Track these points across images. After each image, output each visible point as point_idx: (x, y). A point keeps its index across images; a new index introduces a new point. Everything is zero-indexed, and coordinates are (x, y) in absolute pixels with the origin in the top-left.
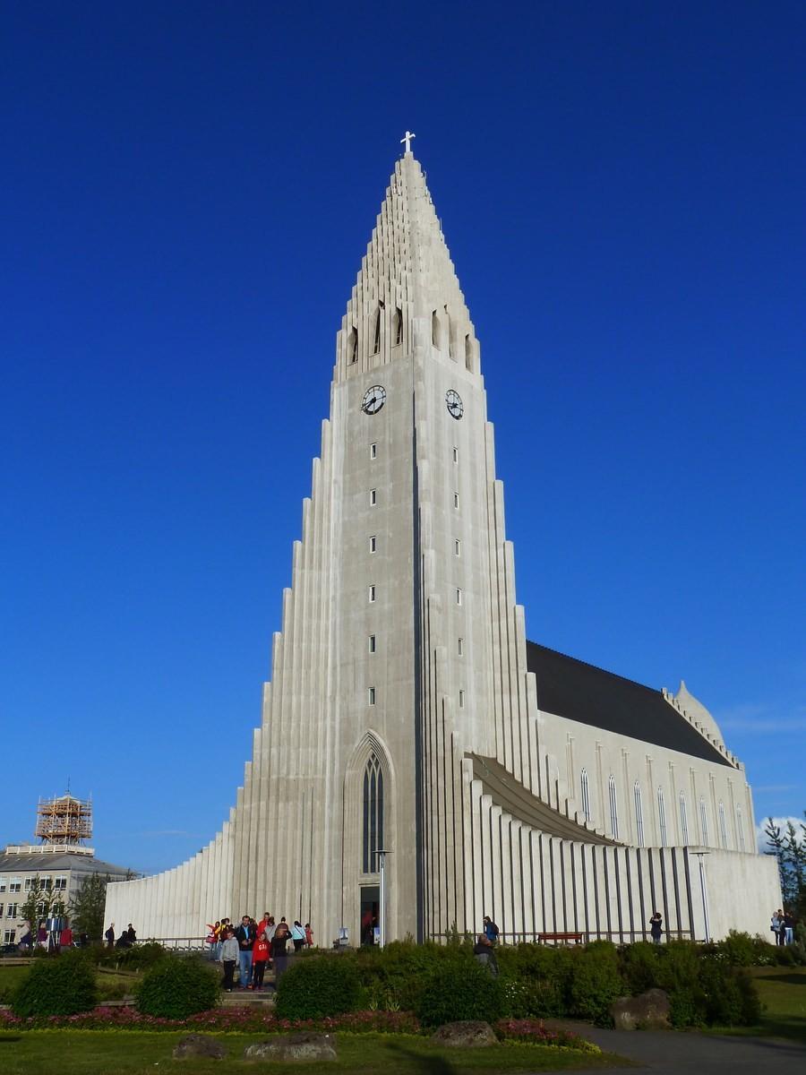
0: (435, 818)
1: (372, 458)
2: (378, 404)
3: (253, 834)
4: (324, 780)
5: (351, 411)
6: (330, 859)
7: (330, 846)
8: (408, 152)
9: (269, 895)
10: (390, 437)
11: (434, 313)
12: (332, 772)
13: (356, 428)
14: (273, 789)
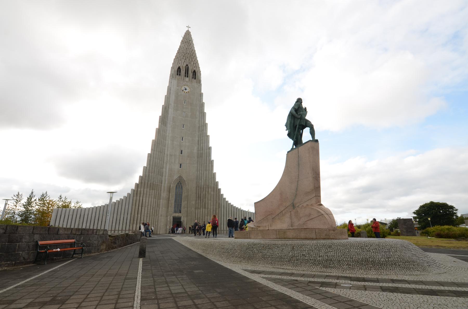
2: (187, 91)
3: (141, 198)
5: (178, 88)
6: (162, 208)
13: (179, 93)
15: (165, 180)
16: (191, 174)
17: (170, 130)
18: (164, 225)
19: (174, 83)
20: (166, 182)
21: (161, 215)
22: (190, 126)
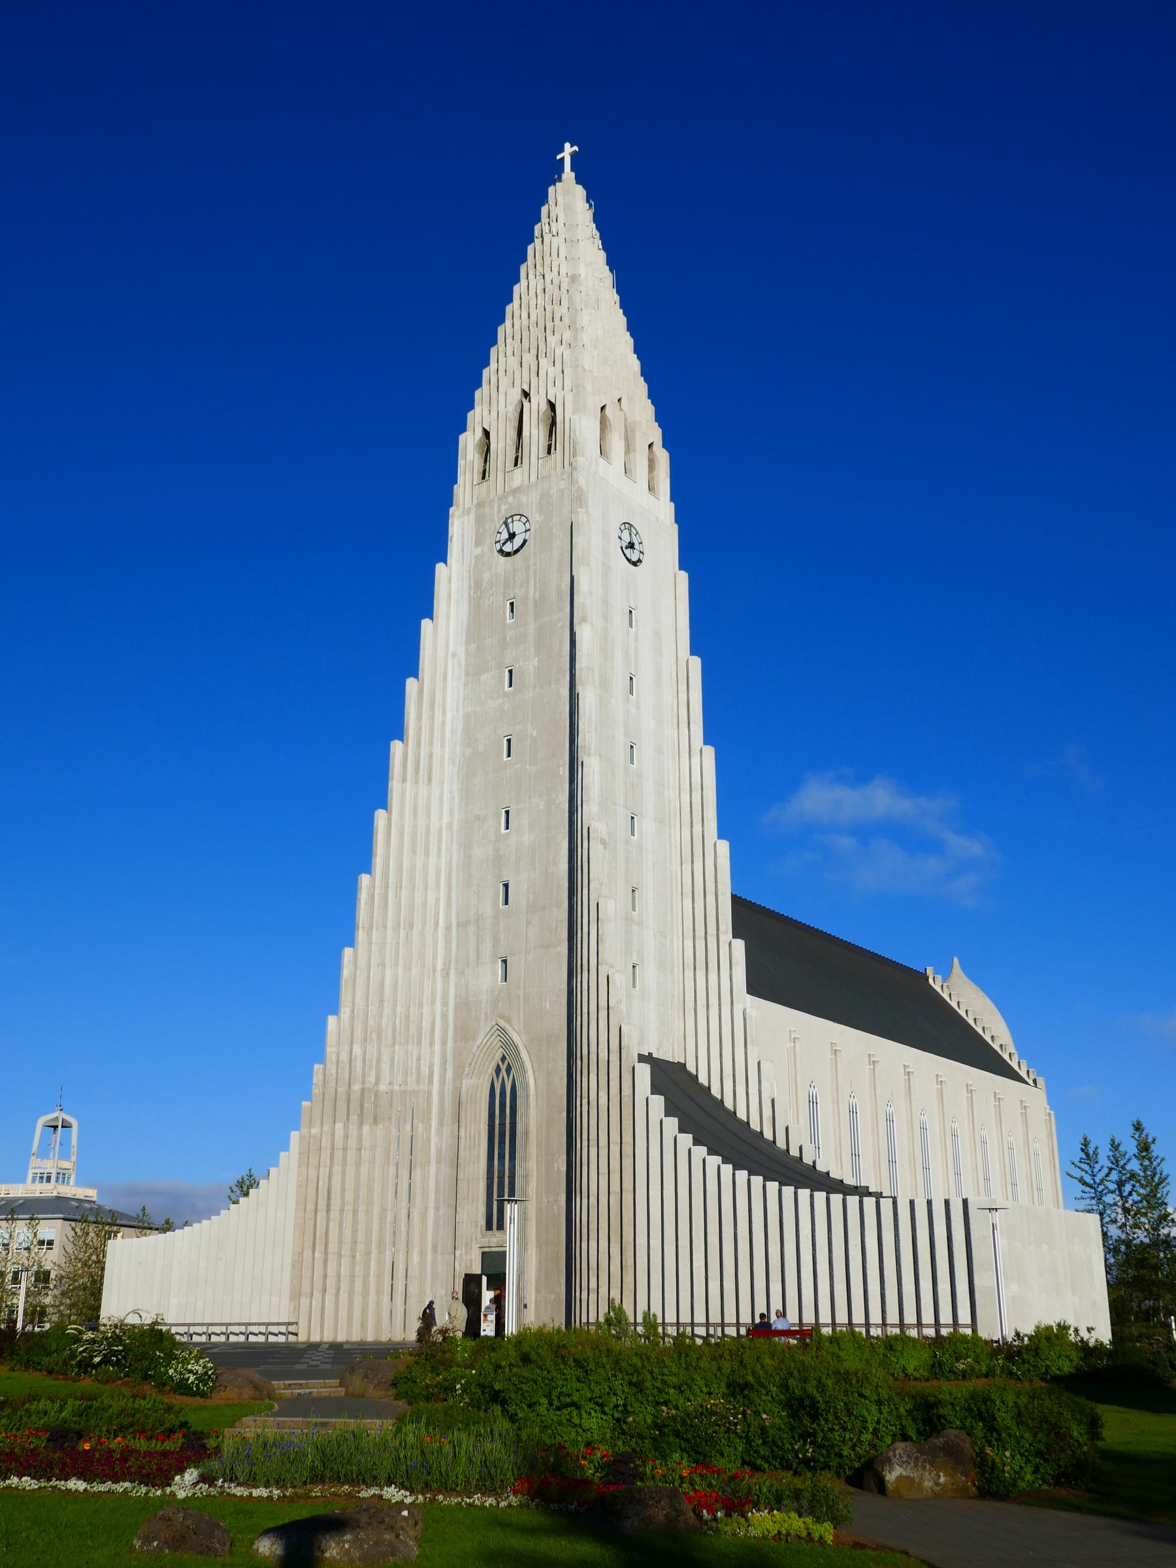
0: (593, 1150)
1: (508, 621)
2: (518, 542)
3: (324, 1172)
4: (430, 1093)
5: (478, 551)
6: (437, 1209)
7: (437, 1191)
8: (568, 174)
9: (345, 1262)
10: (535, 586)
11: (603, 408)
12: (443, 1081)
13: (486, 576)
14: (354, 1105)
15: (445, 1063)
16: (548, 1007)
17: (456, 793)
18: (446, 1294)
19: (463, 535)
20: (449, 1074)
21: (435, 1247)
22: (535, 733)
